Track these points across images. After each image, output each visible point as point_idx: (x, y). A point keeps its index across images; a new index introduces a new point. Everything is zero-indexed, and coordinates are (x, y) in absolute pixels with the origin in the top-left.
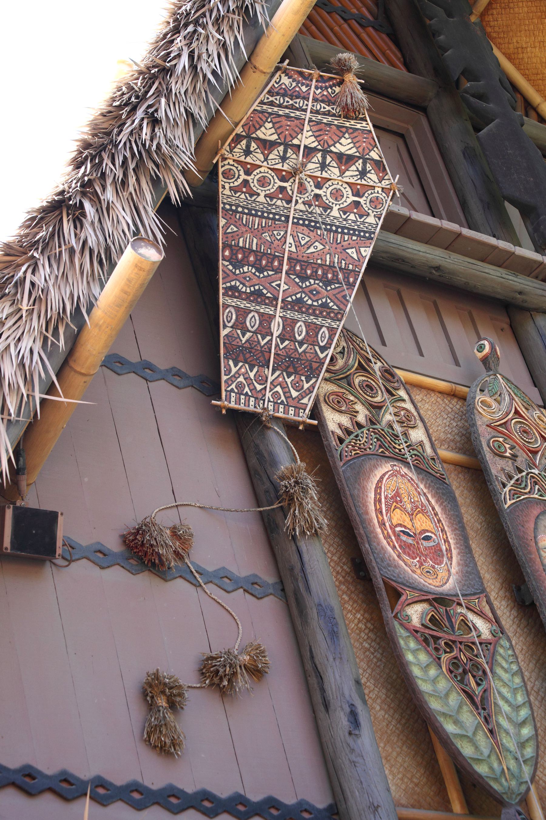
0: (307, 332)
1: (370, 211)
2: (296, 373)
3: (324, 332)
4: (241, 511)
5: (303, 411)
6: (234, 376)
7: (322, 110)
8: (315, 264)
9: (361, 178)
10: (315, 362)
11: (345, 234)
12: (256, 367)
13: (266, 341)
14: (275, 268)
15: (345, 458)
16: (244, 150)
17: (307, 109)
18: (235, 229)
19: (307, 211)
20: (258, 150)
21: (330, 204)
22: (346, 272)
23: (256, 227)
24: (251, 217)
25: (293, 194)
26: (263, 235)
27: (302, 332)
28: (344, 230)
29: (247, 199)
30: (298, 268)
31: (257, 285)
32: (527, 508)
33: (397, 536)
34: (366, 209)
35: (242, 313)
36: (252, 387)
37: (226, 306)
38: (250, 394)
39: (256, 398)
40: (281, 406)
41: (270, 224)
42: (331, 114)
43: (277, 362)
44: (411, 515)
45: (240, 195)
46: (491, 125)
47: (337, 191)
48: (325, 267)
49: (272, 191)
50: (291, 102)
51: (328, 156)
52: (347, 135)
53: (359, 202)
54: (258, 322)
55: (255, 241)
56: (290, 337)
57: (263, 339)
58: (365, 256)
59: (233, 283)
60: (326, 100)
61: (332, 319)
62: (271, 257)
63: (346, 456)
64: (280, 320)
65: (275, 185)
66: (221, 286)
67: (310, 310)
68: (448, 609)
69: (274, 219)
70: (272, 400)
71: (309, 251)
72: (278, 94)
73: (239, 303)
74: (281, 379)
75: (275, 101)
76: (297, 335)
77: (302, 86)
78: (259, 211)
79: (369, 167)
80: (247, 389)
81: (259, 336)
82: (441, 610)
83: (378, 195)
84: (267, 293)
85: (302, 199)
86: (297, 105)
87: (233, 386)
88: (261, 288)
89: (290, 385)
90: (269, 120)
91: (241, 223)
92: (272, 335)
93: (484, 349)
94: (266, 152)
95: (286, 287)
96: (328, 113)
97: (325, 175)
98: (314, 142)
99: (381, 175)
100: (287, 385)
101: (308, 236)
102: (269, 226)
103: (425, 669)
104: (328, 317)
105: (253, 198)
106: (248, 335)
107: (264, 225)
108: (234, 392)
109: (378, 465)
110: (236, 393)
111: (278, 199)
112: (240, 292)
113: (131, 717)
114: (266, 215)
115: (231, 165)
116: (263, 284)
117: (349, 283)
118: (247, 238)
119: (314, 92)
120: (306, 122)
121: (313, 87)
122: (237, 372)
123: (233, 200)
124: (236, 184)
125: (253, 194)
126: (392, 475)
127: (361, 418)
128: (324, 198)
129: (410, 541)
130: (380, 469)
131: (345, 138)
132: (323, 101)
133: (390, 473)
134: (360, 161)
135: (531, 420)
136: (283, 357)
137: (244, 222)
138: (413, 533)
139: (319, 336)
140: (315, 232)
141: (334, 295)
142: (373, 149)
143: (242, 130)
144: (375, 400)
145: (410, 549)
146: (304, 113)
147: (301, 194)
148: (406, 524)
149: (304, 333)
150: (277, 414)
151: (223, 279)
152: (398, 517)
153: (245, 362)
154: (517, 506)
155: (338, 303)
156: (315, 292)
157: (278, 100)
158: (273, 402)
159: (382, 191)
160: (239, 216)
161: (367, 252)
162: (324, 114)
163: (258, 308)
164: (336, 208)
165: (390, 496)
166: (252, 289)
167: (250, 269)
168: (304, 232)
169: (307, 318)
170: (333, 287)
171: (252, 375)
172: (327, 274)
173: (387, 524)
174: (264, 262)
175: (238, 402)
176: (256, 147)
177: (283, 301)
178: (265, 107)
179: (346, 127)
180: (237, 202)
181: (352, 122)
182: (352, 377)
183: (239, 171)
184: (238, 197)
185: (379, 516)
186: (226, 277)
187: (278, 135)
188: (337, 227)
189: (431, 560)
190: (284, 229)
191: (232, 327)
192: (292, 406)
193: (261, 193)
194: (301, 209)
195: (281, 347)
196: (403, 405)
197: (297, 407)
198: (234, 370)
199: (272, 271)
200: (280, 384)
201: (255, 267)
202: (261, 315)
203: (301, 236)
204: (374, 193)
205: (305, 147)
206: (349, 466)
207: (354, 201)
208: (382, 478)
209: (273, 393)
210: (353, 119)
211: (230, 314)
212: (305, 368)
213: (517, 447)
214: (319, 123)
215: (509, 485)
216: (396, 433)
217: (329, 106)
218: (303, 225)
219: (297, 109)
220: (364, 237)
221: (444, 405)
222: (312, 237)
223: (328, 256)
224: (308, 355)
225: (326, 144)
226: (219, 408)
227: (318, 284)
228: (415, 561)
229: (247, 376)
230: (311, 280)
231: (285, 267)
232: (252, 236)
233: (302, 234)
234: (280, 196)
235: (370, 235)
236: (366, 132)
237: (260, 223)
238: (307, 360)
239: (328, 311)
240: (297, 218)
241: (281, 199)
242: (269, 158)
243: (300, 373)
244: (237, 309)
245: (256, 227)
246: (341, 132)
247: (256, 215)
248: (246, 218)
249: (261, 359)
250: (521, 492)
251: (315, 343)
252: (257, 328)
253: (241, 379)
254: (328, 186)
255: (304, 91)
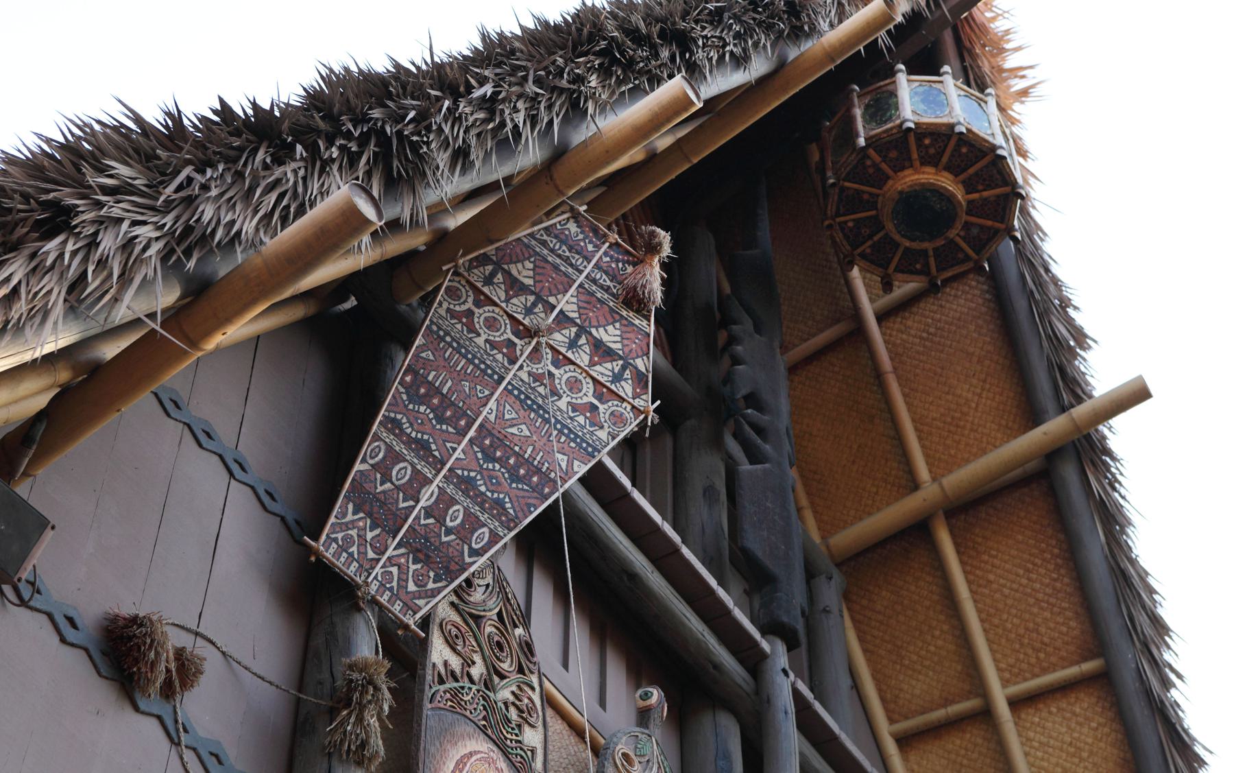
1: (605, 424)
3: (483, 533)
4: (277, 686)
5: (412, 614)
6: (346, 524)
7: (601, 281)
8: (511, 448)
9: (612, 382)
10: (456, 563)
11: (564, 434)
12: (379, 530)
13: (406, 504)
15: (436, 702)
16: (485, 276)
17: (583, 271)
18: (431, 357)
19: (529, 384)
20: (503, 286)
21: (561, 391)
22: (546, 479)
23: (458, 368)
24: (457, 356)
25: (521, 355)
26: (463, 383)
27: (456, 518)
29: (462, 332)
30: (487, 442)
31: (427, 434)
34: (603, 420)
35: (394, 457)
36: (362, 550)
37: (377, 438)
38: (356, 556)
39: (361, 566)
40: (387, 592)
41: (477, 375)
42: (610, 291)
45: (456, 323)
46: (759, 466)
47: (576, 381)
49: (497, 339)
50: (567, 254)
51: (584, 336)
52: (617, 325)
53: (597, 408)
54: (407, 478)
55: (449, 383)
57: (403, 501)
58: (577, 472)
59: (399, 417)
60: (611, 273)
61: (501, 522)
63: (439, 701)
64: (436, 490)
65: (505, 335)
66: (382, 412)
67: (480, 499)
69: (484, 372)
70: (380, 579)
71: (510, 430)
72: (556, 237)
73: (394, 443)
74: (403, 560)
75: (549, 242)
76: (448, 519)
77: (589, 243)
78: (470, 352)
79: (627, 374)
80: (354, 549)
81: (401, 495)
83: (624, 411)
84: (435, 451)
85: (530, 368)
86: (574, 261)
87: (340, 536)
88: (431, 440)
89: (411, 574)
90: (532, 259)
91: (442, 355)
92: (417, 501)
93: (649, 698)
94: (511, 293)
95: (462, 456)
96: (607, 290)
97: (569, 355)
98: (575, 312)
99: (638, 390)
100: (408, 571)
101: (516, 413)
102: (474, 376)
104: (497, 518)
105: (470, 336)
106: (388, 486)
107: (469, 371)
108: (337, 543)
109: (473, 737)
110: (339, 545)
111: (500, 352)
112: (402, 430)
113: (178, 418)
114: (477, 361)
115: (462, 285)
116: (435, 437)
117: (543, 493)
118: (441, 375)
119: (601, 257)
120: (576, 285)
121: (602, 250)
122: (353, 522)
123: (445, 324)
124: (457, 308)
125: (472, 329)
128: (557, 381)
130: (474, 742)
131: (614, 326)
132: (606, 273)
133: (483, 755)
134: (621, 362)
136: (419, 536)
137: (447, 355)
139: (476, 535)
140: (528, 413)
141: (517, 497)
142: (642, 356)
143: (494, 253)
144: (502, 665)
146: (577, 274)
147: (530, 361)
149: (459, 521)
150: (378, 598)
151: (389, 404)
153: (369, 514)
156: (494, 481)
157: (553, 242)
158: (380, 582)
159: (631, 409)
160: (444, 346)
162: (602, 287)
163: (416, 461)
164: (565, 399)
166: (419, 436)
167: (427, 412)
169: (471, 506)
170: (520, 486)
171: (369, 535)
174: (449, 413)
175: (337, 555)
176: (501, 280)
177: (450, 470)
178: (533, 242)
179: (622, 316)
180: (449, 329)
181: (631, 314)
182: (484, 621)
183: (467, 296)
184: (452, 324)
186: (393, 405)
187: (535, 282)
190: (492, 390)
191: (372, 466)
192: (401, 600)
193: (482, 334)
194: (522, 377)
195: (423, 522)
197: (407, 605)
198: (350, 517)
199: (454, 428)
201: (434, 413)
202: (416, 472)
203: (508, 407)
204: (621, 406)
205: (561, 311)
207: (591, 403)
208: (471, 754)
209: (385, 571)
210: (633, 311)
211: (377, 450)
212: (439, 563)
214: (592, 294)
216: (509, 717)
217: (611, 281)
218: (517, 397)
219: (571, 265)
221: (568, 742)
224: (451, 550)
225: (587, 322)
226: (309, 550)
227: (503, 474)
229: (362, 533)
230: (496, 464)
232: (447, 377)
233: (511, 406)
234: (505, 350)
235: (593, 452)
236: (643, 333)
237: (465, 367)
238: (447, 556)
240: (513, 385)
241: (504, 354)
242: (511, 301)
243: (432, 566)
244: (389, 448)
245: (458, 368)
246: (613, 317)
247: (465, 356)
248: (451, 353)
249: (391, 523)
251: (465, 539)
252: (403, 484)
253: (354, 533)
254: (567, 370)
255: (589, 250)
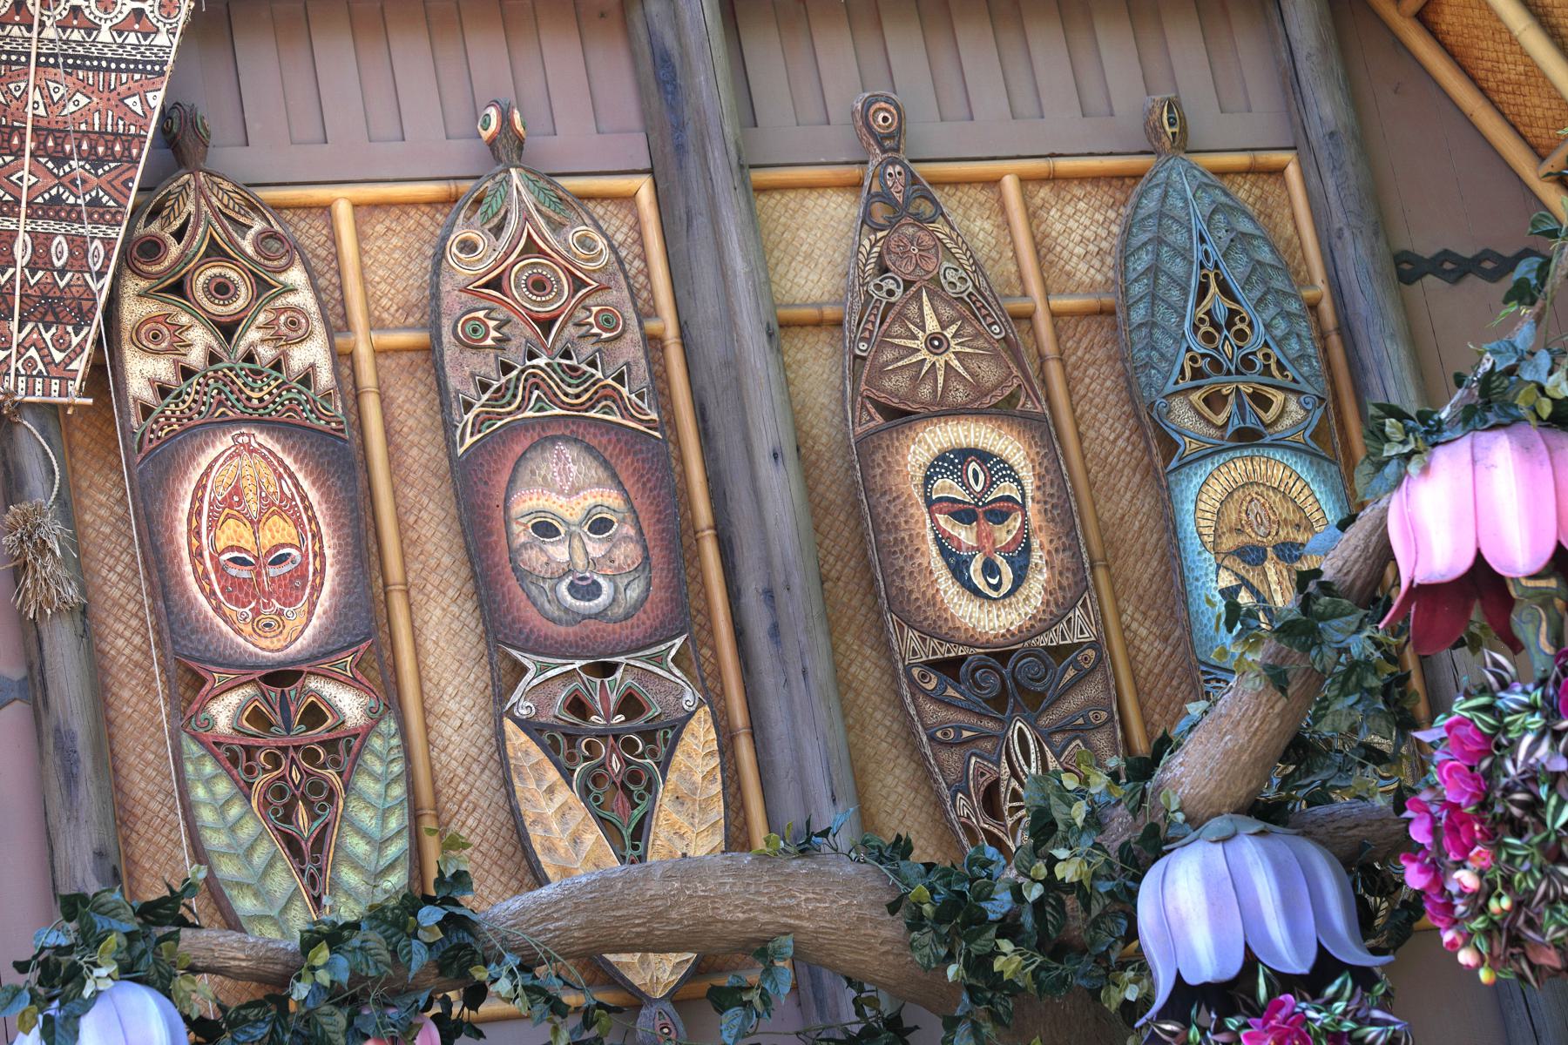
0: (71, 253)
1: (160, 25)
2: (58, 321)
14: (14, 150)
19: (61, 40)
21: (97, 21)
22: (128, 140)
27: (62, 253)
28: (120, 64)
30: (51, 143)
32: (504, 443)
33: (220, 570)
34: (154, 21)
40: (38, 380)
43: (28, 308)
44: (255, 524)
48: (93, 136)
53: (142, 10)
56: (45, 264)
61: (108, 223)
62: (7, 130)
63: (151, 440)
64: (27, 238)
67: (73, 214)
68: (286, 689)
70: (23, 372)
74: (35, 336)
82: (273, 694)
95: (34, 180)
103: (222, 809)
126: (231, 457)
127: (196, 357)
128: (87, 12)
129: (244, 573)
135: (557, 252)
138: (254, 557)
141: (109, 182)
145: (241, 589)
148: (242, 544)
149: (66, 254)
152: (233, 533)
154: (484, 445)
155: (116, 195)
161: (156, 100)
164: (105, 27)
165: (220, 498)
168: (57, 78)
170: (106, 168)
172: (95, 148)
173: (206, 554)
185: (194, 541)
188: (109, 61)
189: (278, 600)
195: (32, 282)
196: (292, 299)
200: (34, 345)
203: (52, 85)
206: (152, 460)
213: (515, 318)
215: (478, 404)
220: (153, 72)
222: (71, 85)
223: (97, 115)
224: (74, 289)
227: (83, 167)
228: (247, 610)
231: (29, 145)
234: (17, 18)
238: (74, 298)
239: (101, 210)
241: (18, 24)
250: (499, 414)
